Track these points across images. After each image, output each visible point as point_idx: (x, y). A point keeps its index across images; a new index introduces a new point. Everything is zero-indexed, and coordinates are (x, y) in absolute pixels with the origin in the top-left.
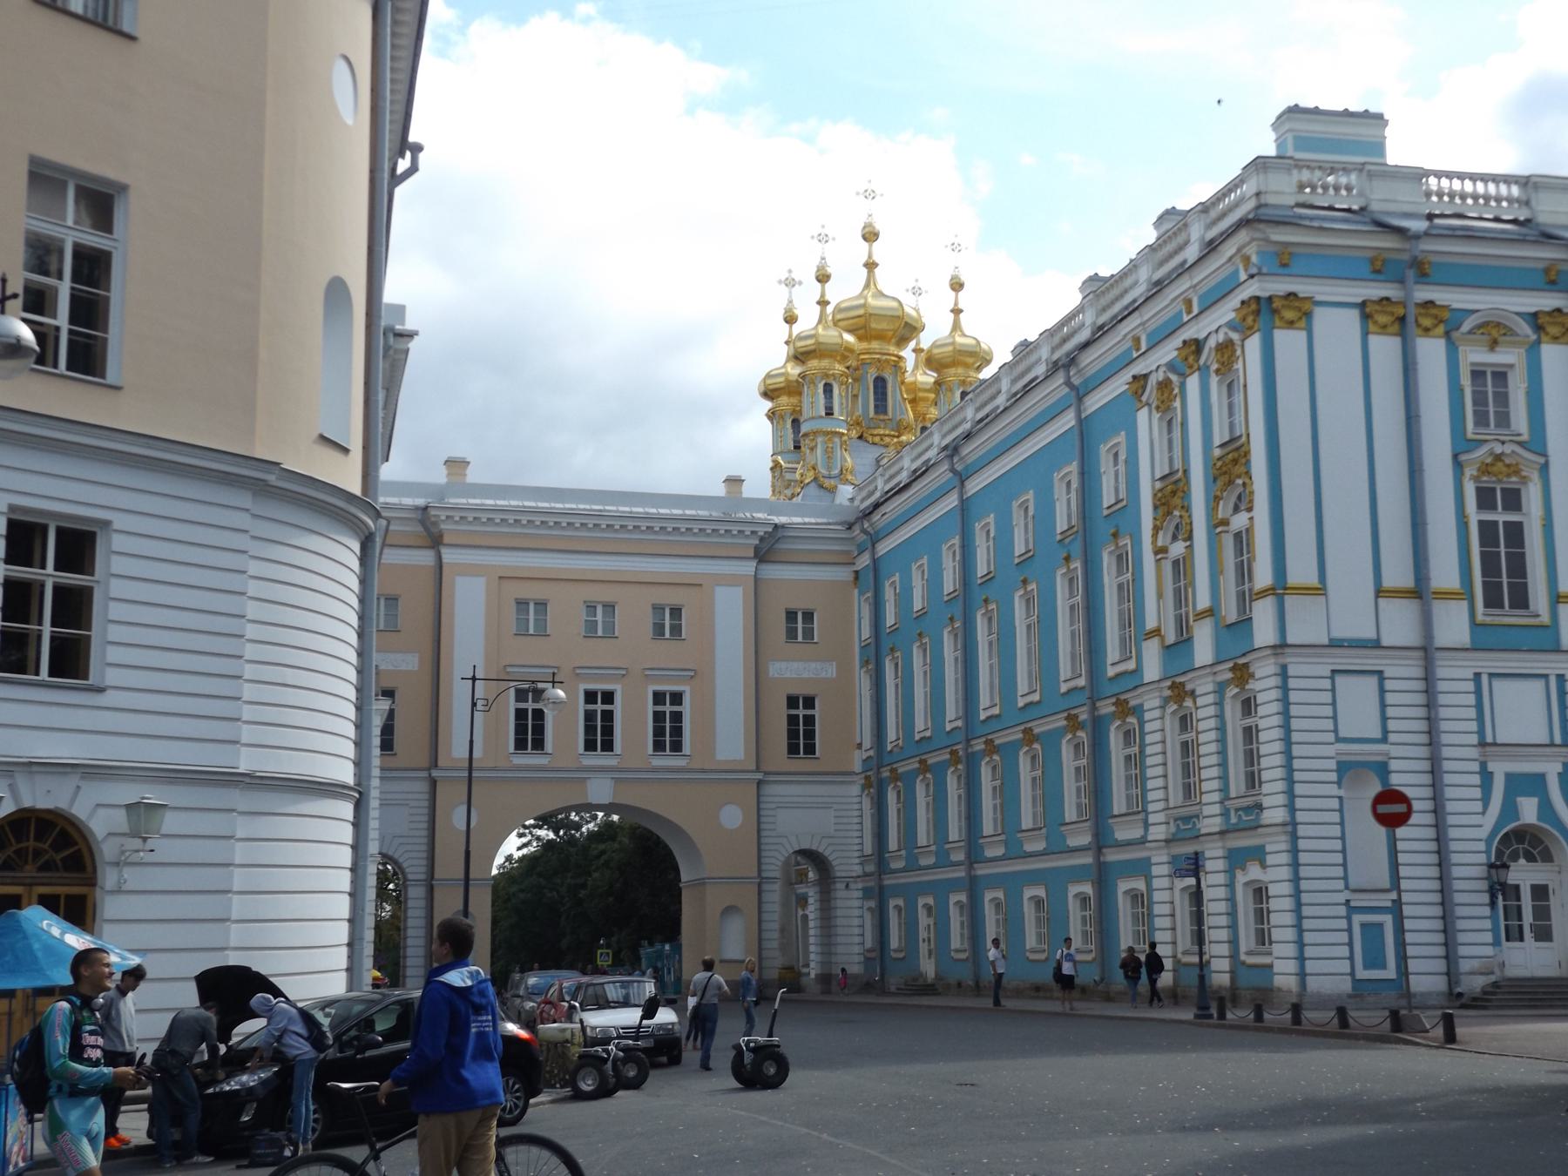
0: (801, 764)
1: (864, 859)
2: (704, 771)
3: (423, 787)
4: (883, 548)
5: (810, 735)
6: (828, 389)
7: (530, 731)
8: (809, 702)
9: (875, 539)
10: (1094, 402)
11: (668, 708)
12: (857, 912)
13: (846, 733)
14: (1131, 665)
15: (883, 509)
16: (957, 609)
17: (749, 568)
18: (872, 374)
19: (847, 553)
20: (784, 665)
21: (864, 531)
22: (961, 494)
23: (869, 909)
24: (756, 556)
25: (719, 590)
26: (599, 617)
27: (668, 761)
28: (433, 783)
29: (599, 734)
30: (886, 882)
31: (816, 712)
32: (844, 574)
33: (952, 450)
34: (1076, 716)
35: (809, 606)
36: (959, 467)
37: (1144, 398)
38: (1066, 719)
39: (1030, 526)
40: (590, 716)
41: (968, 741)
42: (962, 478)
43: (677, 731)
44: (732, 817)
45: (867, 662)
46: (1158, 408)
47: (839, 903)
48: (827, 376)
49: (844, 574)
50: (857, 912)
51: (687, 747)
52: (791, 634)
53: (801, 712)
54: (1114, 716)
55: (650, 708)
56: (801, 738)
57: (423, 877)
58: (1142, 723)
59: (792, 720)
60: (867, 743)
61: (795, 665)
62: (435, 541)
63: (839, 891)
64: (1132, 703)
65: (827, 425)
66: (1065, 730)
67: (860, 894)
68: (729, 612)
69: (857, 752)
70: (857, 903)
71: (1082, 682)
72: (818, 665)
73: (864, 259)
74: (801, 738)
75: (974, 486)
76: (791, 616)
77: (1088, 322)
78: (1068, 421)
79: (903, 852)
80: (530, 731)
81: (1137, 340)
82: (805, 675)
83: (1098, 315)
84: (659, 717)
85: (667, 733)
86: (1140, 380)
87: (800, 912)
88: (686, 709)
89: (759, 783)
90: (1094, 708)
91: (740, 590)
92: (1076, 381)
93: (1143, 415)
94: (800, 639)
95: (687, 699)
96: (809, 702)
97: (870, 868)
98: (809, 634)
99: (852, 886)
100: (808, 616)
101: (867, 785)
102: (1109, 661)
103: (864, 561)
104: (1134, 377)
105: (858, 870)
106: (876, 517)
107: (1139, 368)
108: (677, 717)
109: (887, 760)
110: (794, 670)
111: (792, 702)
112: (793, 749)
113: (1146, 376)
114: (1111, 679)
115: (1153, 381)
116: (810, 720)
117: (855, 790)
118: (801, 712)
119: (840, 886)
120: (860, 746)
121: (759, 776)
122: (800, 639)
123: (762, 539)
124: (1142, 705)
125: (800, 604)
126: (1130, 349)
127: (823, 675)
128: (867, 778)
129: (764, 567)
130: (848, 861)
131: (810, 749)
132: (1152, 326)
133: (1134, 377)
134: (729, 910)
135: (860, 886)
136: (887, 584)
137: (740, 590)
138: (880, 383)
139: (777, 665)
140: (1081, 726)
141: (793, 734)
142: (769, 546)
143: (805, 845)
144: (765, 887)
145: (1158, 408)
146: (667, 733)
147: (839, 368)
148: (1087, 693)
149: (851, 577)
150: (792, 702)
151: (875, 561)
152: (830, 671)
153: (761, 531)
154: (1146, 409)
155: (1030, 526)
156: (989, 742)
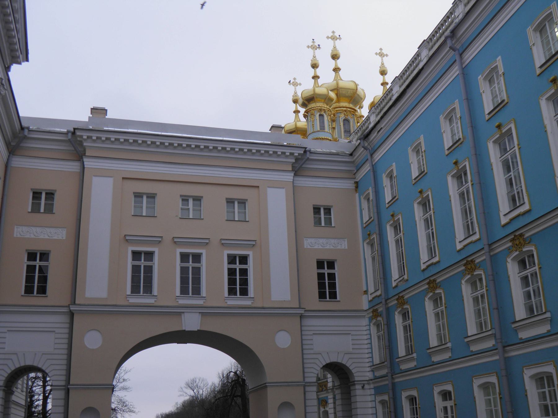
0: (328, 305)
1: (374, 368)
2: (263, 308)
3: (65, 319)
4: (378, 156)
5: (333, 286)
6: (321, 116)
7: (142, 280)
8: (331, 264)
11: (238, 266)
12: (370, 405)
13: (359, 282)
17: (289, 177)
18: (342, 116)
19: (349, 171)
20: (313, 240)
21: (365, 148)
23: (383, 402)
24: (293, 170)
25: (270, 191)
27: (238, 301)
28: (72, 315)
29: (190, 282)
30: (396, 380)
32: (349, 185)
35: (327, 203)
40: (184, 271)
41: (490, 245)
43: (245, 282)
44: (283, 340)
47: (358, 399)
48: (321, 110)
50: (370, 405)
52: (318, 222)
55: (226, 266)
56: (327, 287)
57: (63, 383)
59: (321, 276)
60: (371, 289)
61: (321, 241)
62: (79, 155)
63: (358, 391)
65: (322, 135)
67: (373, 392)
68: (276, 204)
70: (369, 398)
72: (336, 241)
73: (333, 67)
74: (327, 287)
76: (317, 210)
79: (415, 355)
80: (142, 280)
82: (328, 247)
84: (232, 272)
85: (238, 282)
87: (322, 409)
88: (251, 266)
89: (302, 317)
91: (283, 191)
94: (323, 224)
95: (251, 261)
96: (331, 264)
97: (384, 372)
98: (329, 222)
99: (366, 386)
100: (328, 211)
101: (375, 314)
105: (370, 375)
108: (244, 272)
111: (320, 264)
112: (322, 295)
116: (332, 277)
117: (365, 322)
118: (326, 271)
119: (358, 387)
120: (366, 292)
121: (302, 311)
122: (323, 224)
123: (297, 159)
125: (322, 202)
127: (339, 247)
128: (375, 311)
129: (296, 178)
130: (361, 371)
131: (333, 295)
134: (286, 405)
135: (372, 386)
136: (384, 176)
137: (283, 191)
138: (346, 121)
139: (310, 240)
141: (321, 285)
142: (301, 162)
143: (334, 359)
144: (308, 389)
146: (238, 282)
147: (325, 106)
149: (353, 186)
150: (320, 264)
152: (344, 245)
153: (297, 152)
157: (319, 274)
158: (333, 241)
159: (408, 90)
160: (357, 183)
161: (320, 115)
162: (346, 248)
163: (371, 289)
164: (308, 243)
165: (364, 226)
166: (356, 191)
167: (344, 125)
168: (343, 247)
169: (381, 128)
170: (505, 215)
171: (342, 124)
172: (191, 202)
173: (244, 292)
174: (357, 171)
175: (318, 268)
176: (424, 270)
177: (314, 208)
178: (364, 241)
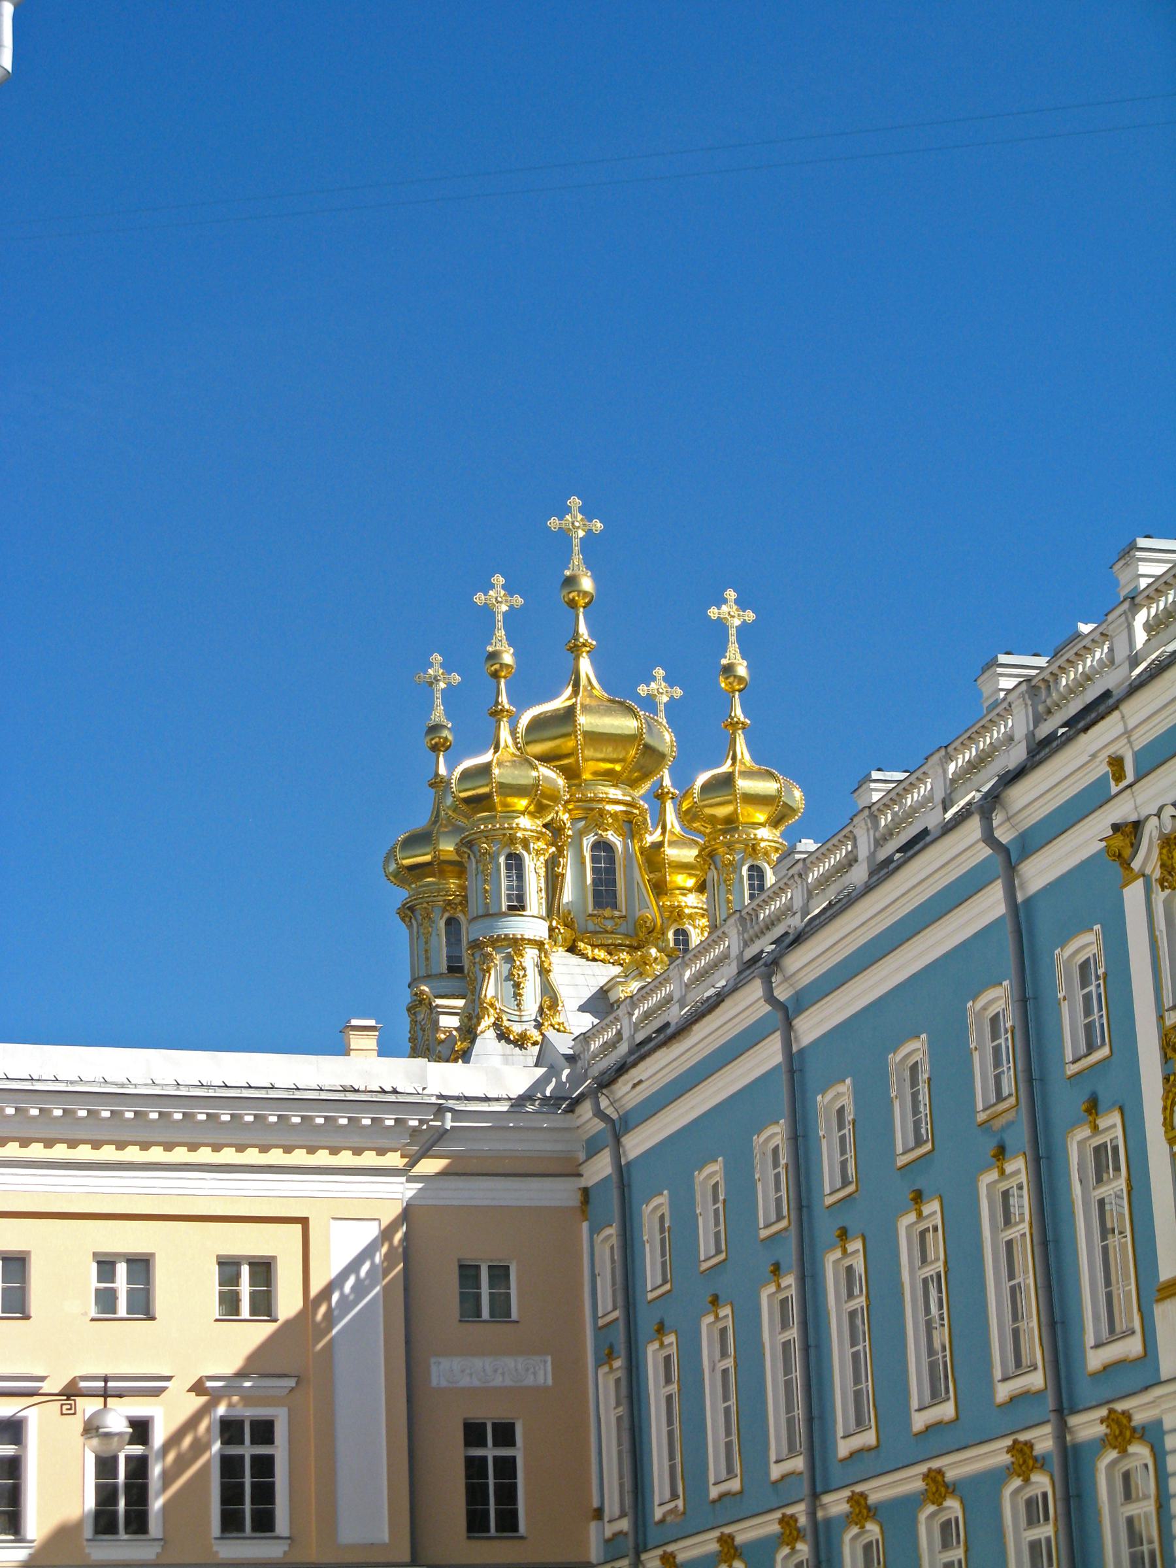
4: (636, 1144)
5: (508, 1494)
9: (618, 1128)
10: (1038, 873)
11: (248, 1450)
14: (1133, 1347)
15: (635, 1074)
16: (789, 1253)
20: (456, 1363)
21: (599, 1113)
22: (787, 1043)
26: (121, 1283)
31: (518, 1453)
32: (562, 1193)
33: (763, 967)
34: (1030, 1445)
36: (782, 994)
37: (1136, 865)
38: (1010, 1450)
39: (924, 1097)
42: (786, 1014)
43: (265, 1493)
45: (610, 1356)
46: (1162, 882)
49: (562, 1193)
51: (282, 1525)
52: (470, 1308)
53: (490, 1452)
54: (1104, 1442)
56: (491, 1501)
58: (1159, 1455)
59: (475, 1467)
60: (612, 1507)
61: (478, 1363)
64: (1139, 1418)
66: (1008, 1472)
69: (593, 1526)
71: (1036, 1380)
75: (811, 1027)
76: (468, 1273)
77: (1020, 733)
78: (991, 904)
81: (1117, 763)
83: (1038, 720)
86: (1131, 830)
88: (280, 1451)
90: (1062, 1430)
92: (1004, 835)
93: (1133, 894)
95: (281, 1432)
96: (505, 1434)
98: (501, 1308)
100: (500, 1274)
102: (1090, 1340)
103: (601, 1168)
104: (1116, 828)
106: (622, 1087)
107: (1121, 810)
108: (264, 1465)
109: (653, 1535)
110: (477, 1373)
111: (474, 1433)
112: (476, 1524)
113: (1137, 826)
114: (1094, 1375)
115: (1151, 830)
116: (506, 1467)
118: (490, 1452)
120: (599, 1514)
124: (1159, 1423)
126: (1101, 782)
127: (530, 1381)
131: (508, 1522)
132: (1142, 739)
133: (1116, 828)
136: (647, 1209)
140: (1041, 1463)
141: (475, 1493)
145: (1162, 882)
148: (1050, 1403)
149: (575, 1200)
150: (474, 1433)
151: (623, 1172)
152: (542, 1373)
154: (1138, 885)
155: (924, 1097)
156: (858, 1500)
157: (470, 1462)
158: (509, 1362)
159: (696, 1028)
160: (586, 1191)
161: (509, 856)
162: (550, 1382)
163: (612, 1507)
164: (446, 1372)
165: (601, 1322)
166: (583, 1212)
167: (594, 859)
168: (541, 1380)
169: (640, 1082)
170: (844, 1437)
171: (588, 855)
172: (122, 1269)
173: (264, 1523)
174: (589, 1157)
175: (468, 1443)
176: (714, 1502)
177: (461, 1267)
178: (598, 1365)
